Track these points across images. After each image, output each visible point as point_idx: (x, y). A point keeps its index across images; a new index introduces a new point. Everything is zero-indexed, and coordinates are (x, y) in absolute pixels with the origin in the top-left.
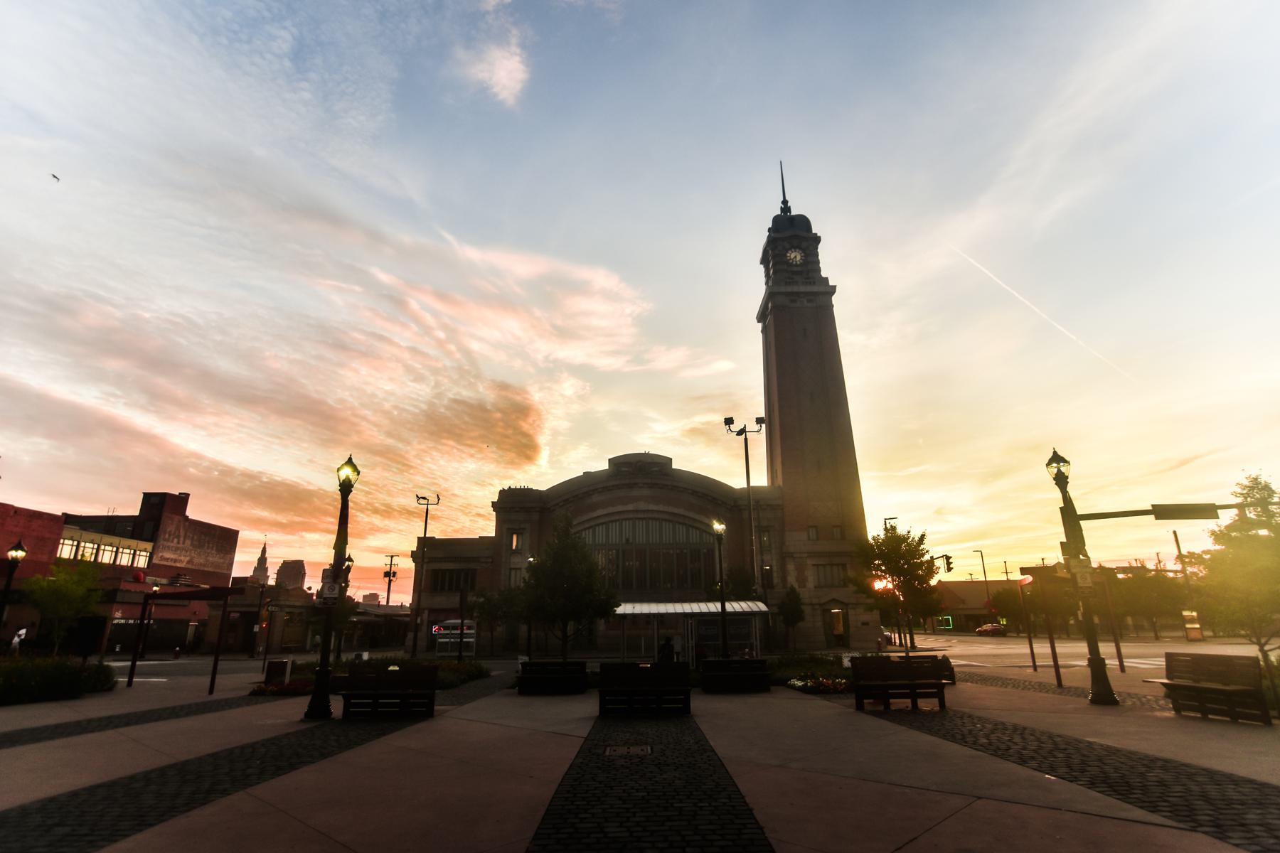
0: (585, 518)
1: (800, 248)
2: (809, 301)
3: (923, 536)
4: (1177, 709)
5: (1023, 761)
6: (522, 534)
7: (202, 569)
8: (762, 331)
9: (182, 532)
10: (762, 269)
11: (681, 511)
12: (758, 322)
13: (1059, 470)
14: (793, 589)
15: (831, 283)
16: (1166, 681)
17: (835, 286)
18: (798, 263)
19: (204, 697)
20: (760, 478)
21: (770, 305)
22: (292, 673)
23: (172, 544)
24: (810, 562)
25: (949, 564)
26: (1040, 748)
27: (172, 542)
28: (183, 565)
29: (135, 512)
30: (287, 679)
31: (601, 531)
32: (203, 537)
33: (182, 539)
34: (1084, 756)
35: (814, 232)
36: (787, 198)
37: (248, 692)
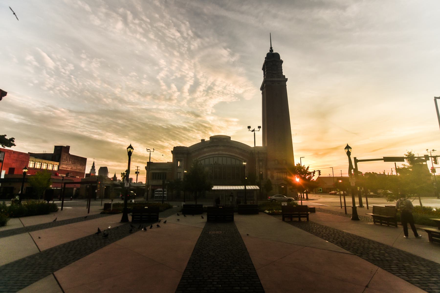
0: (202, 156)
3: (308, 167)
4: (375, 222)
5: (322, 237)
6: (181, 161)
7: (75, 171)
8: (262, 94)
9: (68, 159)
10: (262, 72)
11: (234, 154)
12: (261, 90)
13: (348, 151)
14: (269, 180)
15: (286, 78)
16: (372, 214)
17: (287, 79)
19: (86, 214)
20: (260, 143)
21: (265, 85)
22: (113, 207)
23: (65, 163)
25: (320, 173)
26: (329, 233)
27: (65, 162)
28: (69, 170)
29: (52, 152)
30: (112, 208)
31: (207, 160)
32: (75, 161)
33: (68, 161)
34: (339, 236)
35: (281, 59)
37: (99, 213)
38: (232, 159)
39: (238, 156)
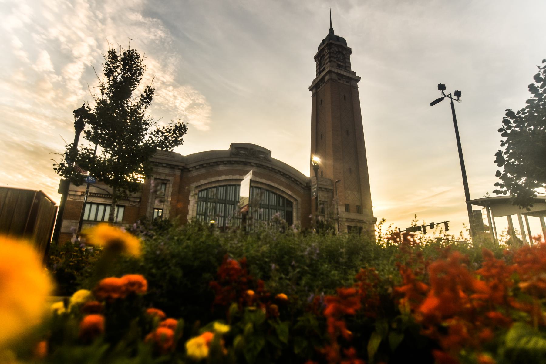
0: (213, 179)
2: (347, 82)
11: (275, 185)
24: (347, 224)
31: (222, 191)
36: (332, 27)
38: (271, 194)
39: (284, 190)
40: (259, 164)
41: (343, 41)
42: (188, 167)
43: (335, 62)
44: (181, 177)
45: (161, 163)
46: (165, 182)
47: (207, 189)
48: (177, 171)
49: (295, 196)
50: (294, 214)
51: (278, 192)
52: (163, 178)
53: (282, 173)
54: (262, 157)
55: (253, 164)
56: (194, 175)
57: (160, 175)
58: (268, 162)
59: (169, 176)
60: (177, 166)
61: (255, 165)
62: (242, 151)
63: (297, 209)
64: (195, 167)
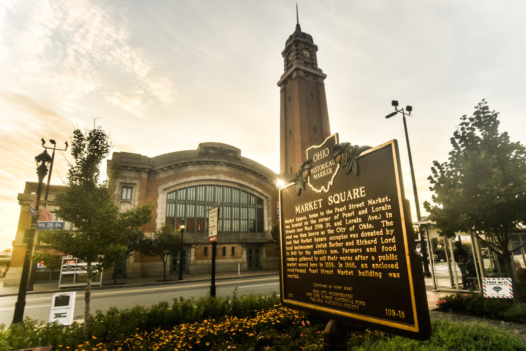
0: (182, 181)
1: (309, 51)
2: (314, 79)
11: (246, 184)
18: (308, 57)
38: (242, 193)
39: (255, 188)
40: (228, 163)
41: (310, 38)
42: (155, 169)
43: (302, 59)
44: (148, 179)
45: (127, 167)
46: (131, 186)
47: (176, 191)
48: (144, 174)
49: (265, 194)
50: (265, 212)
51: (248, 190)
52: (129, 182)
53: (252, 172)
54: (232, 156)
55: (223, 164)
56: (161, 177)
57: (125, 179)
58: (238, 161)
59: (136, 180)
60: (144, 169)
61: (225, 165)
62: (210, 150)
63: (268, 206)
64: (162, 169)
